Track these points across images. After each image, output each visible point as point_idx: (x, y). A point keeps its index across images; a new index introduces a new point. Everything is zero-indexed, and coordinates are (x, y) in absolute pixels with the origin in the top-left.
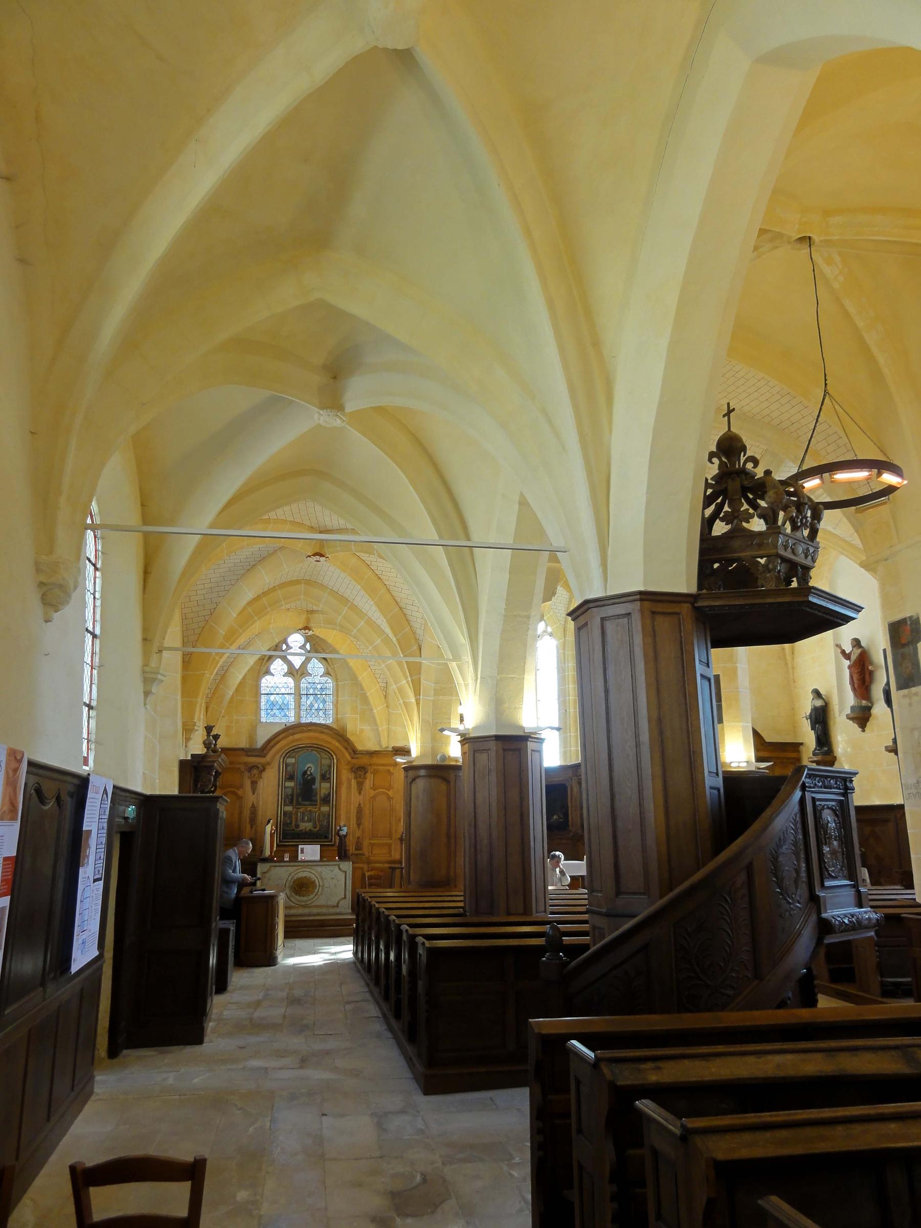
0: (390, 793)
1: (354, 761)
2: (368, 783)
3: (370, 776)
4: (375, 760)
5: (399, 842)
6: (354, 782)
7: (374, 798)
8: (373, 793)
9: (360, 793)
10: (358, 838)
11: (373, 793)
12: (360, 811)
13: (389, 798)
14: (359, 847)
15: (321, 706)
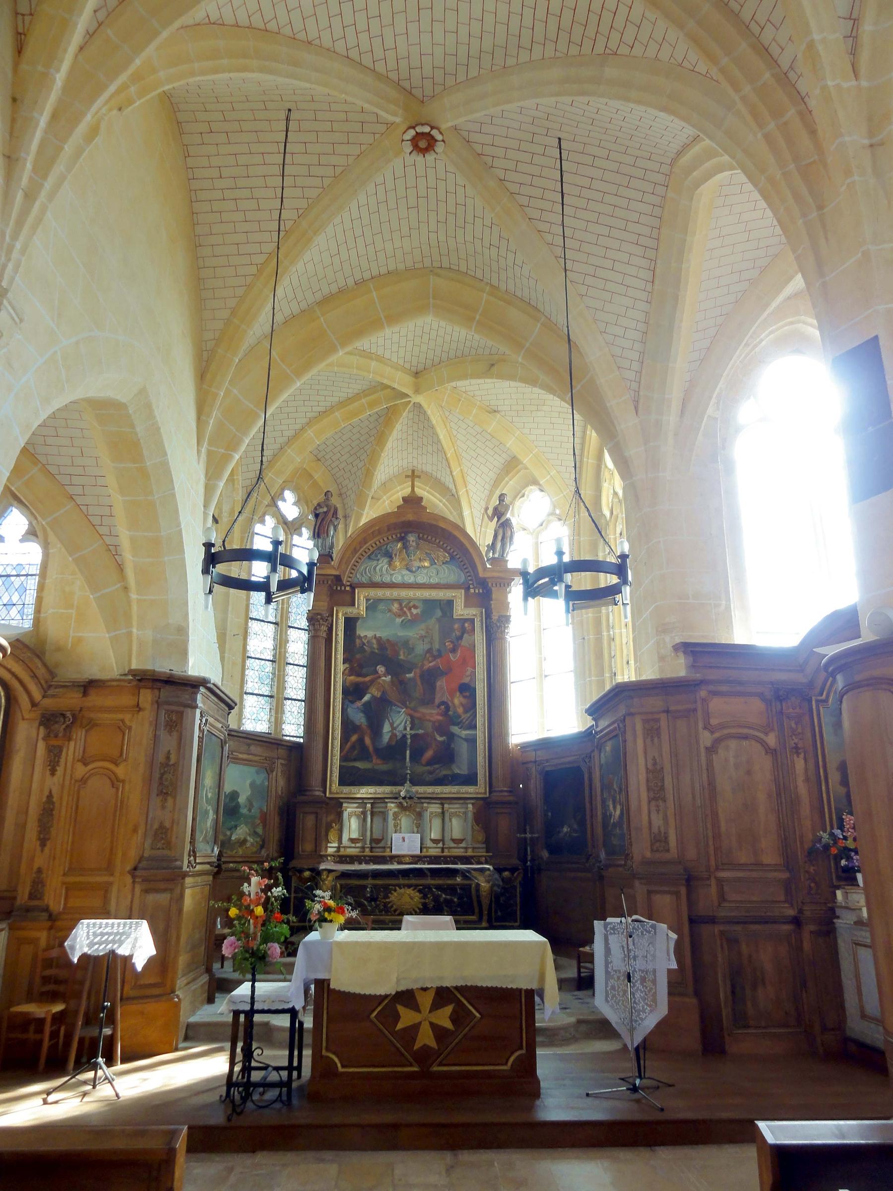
0: (120, 771)
1: (47, 702)
2: (71, 751)
3: (79, 734)
4: (95, 699)
5: (129, 879)
6: (41, 746)
7: (83, 781)
8: (81, 770)
9: (53, 772)
10: (39, 871)
11: (81, 770)
12: (48, 809)
13: (115, 782)
14: (36, 893)
15: (15, 598)
